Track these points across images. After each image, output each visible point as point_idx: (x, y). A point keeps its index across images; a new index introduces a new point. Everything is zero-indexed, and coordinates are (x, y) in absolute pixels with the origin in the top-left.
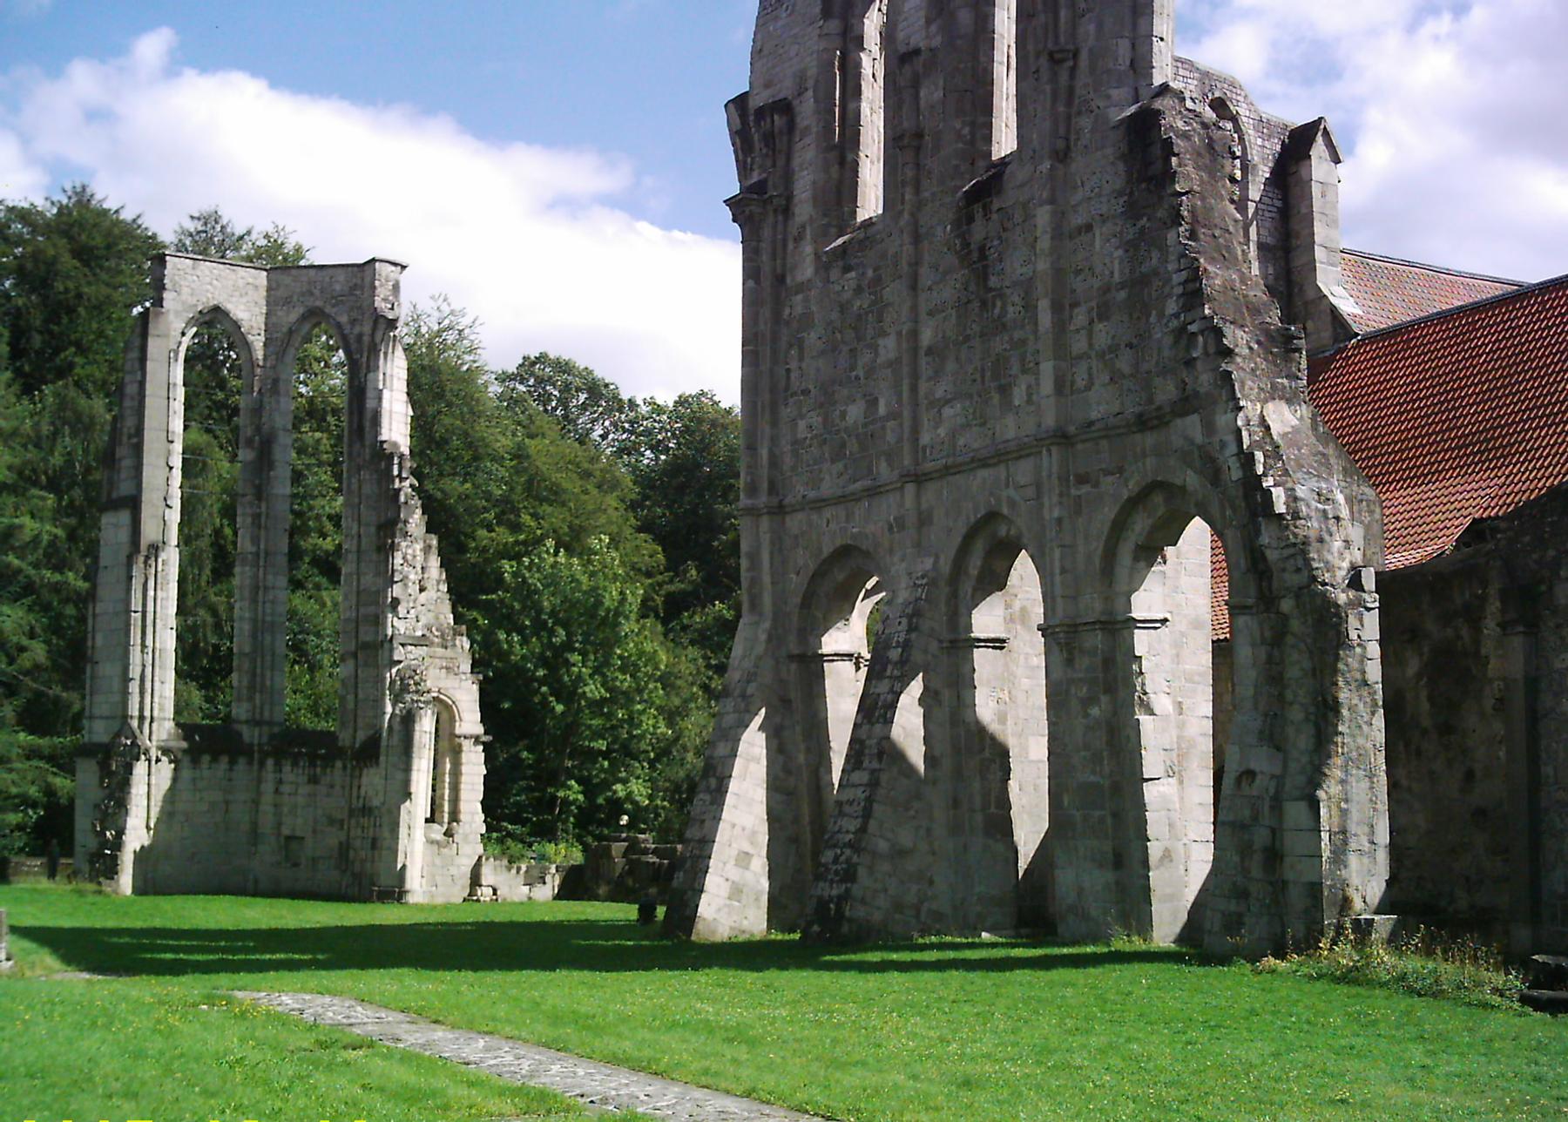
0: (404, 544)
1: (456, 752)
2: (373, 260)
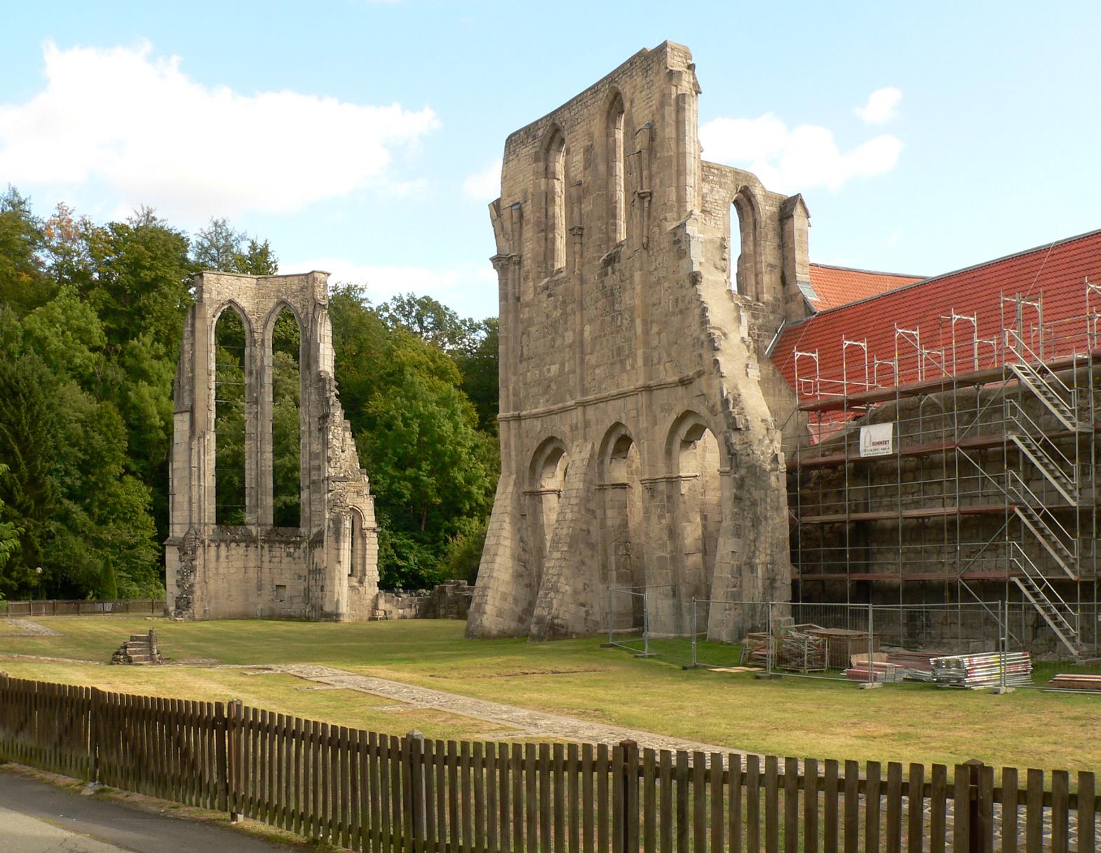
0: (332, 428)
1: (364, 537)
2: (313, 272)
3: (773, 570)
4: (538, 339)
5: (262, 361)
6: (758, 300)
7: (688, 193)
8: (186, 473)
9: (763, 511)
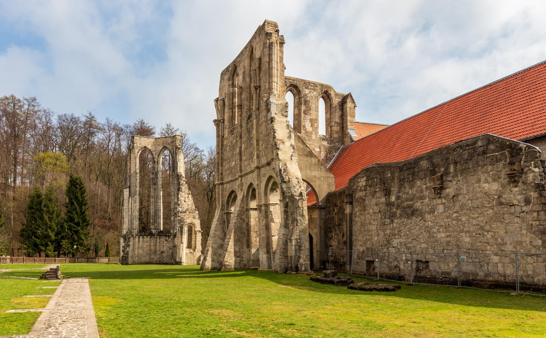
1: (196, 234)
3: (300, 242)
4: (229, 152)
5: (157, 169)
6: (331, 137)
7: (273, 84)
8: (127, 210)
9: (296, 216)
